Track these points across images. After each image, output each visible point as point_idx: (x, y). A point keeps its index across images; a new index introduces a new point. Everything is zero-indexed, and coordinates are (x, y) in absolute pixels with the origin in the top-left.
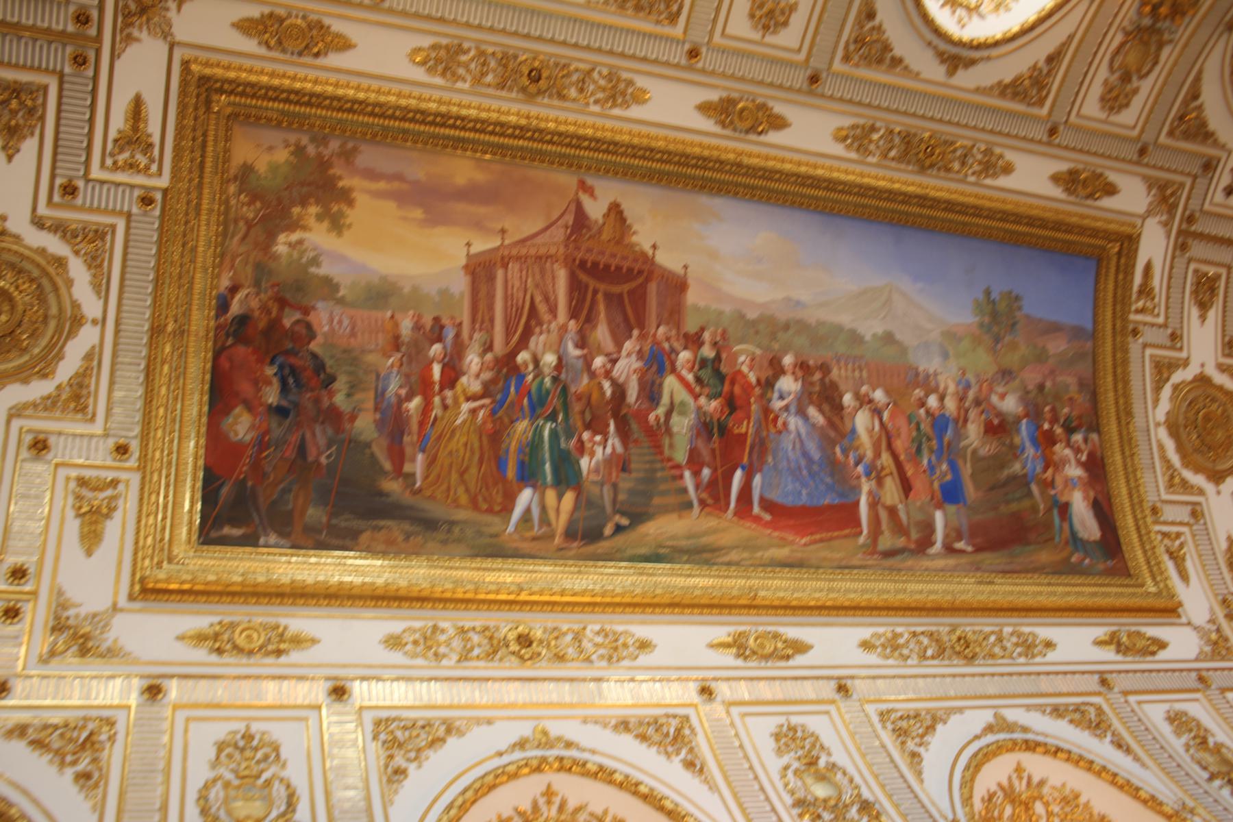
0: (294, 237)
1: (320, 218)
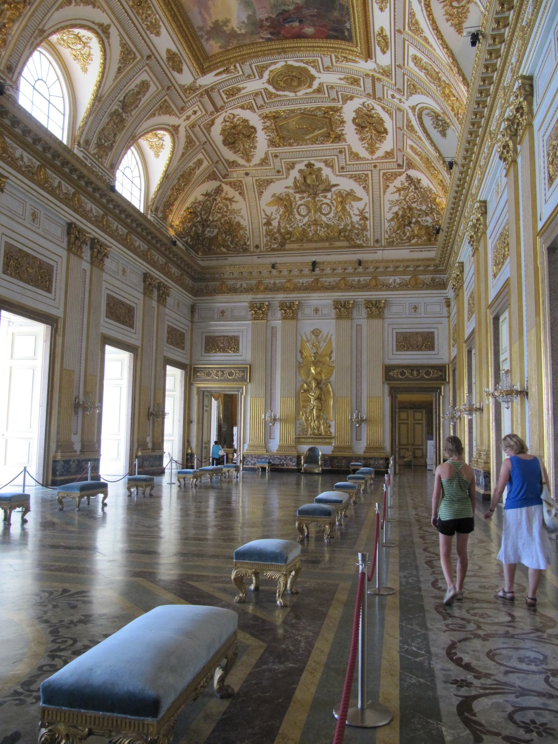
0: (237, 30)
1: (227, 26)
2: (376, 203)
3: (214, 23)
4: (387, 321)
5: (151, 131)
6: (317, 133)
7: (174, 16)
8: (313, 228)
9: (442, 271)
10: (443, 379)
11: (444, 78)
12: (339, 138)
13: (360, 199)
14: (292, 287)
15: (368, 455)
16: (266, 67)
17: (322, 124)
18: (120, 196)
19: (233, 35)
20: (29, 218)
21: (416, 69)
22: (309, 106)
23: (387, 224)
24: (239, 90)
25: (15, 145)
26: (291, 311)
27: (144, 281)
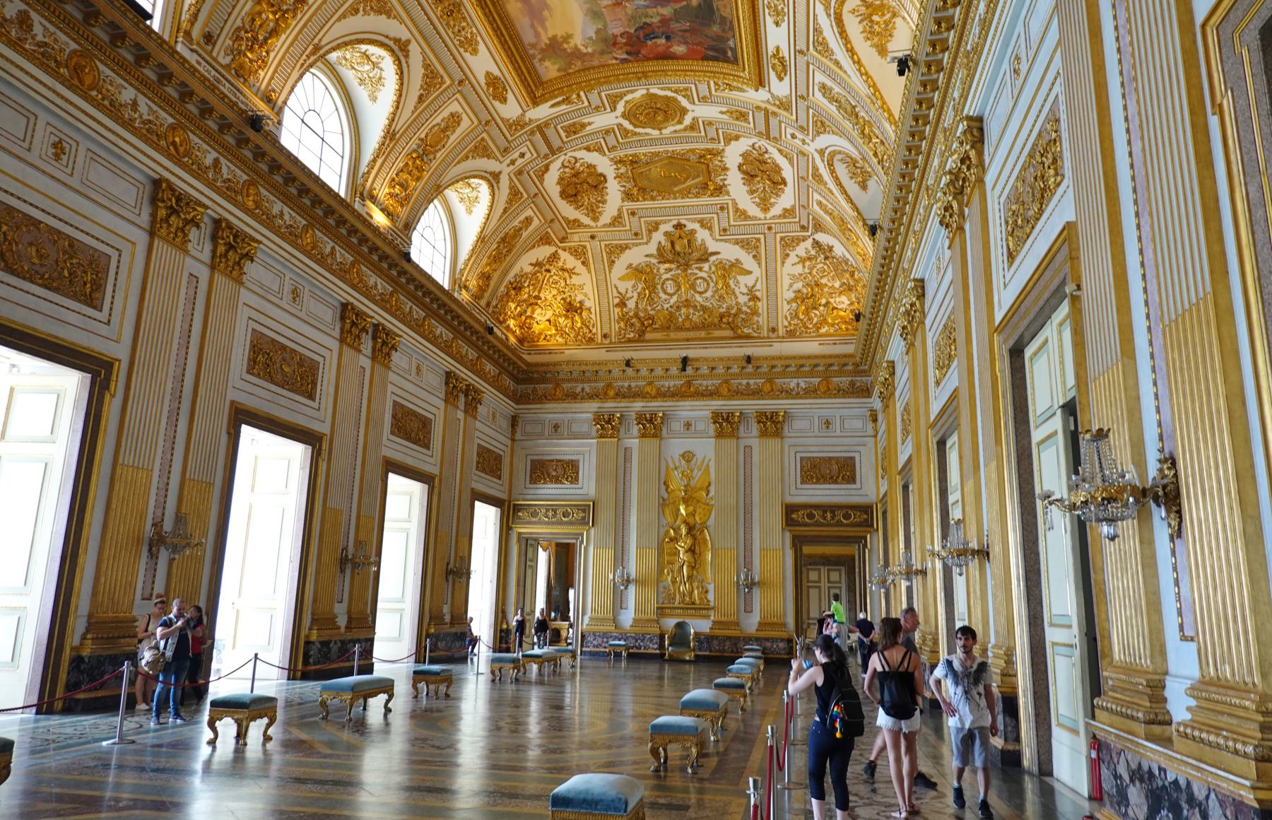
2: (771, 277)
3: (550, 39)
4: (788, 441)
5: (462, 179)
6: (689, 183)
7: (496, 30)
8: (683, 310)
9: (864, 371)
10: (868, 524)
11: (862, 114)
12: (720, 190)
13: (751, 273)
14: (654, 393)
15: (762, 634)
16: (621, 96)
17: (699, 173)
18: (417, 267)
19: (577, 54)
20: (287, 296)
21: (825, 101)
22: (678, 148)
23: (786, 307)
24: (583, 126)
25: (272, 198)
26: (652, 426)
27: (447, 383)
